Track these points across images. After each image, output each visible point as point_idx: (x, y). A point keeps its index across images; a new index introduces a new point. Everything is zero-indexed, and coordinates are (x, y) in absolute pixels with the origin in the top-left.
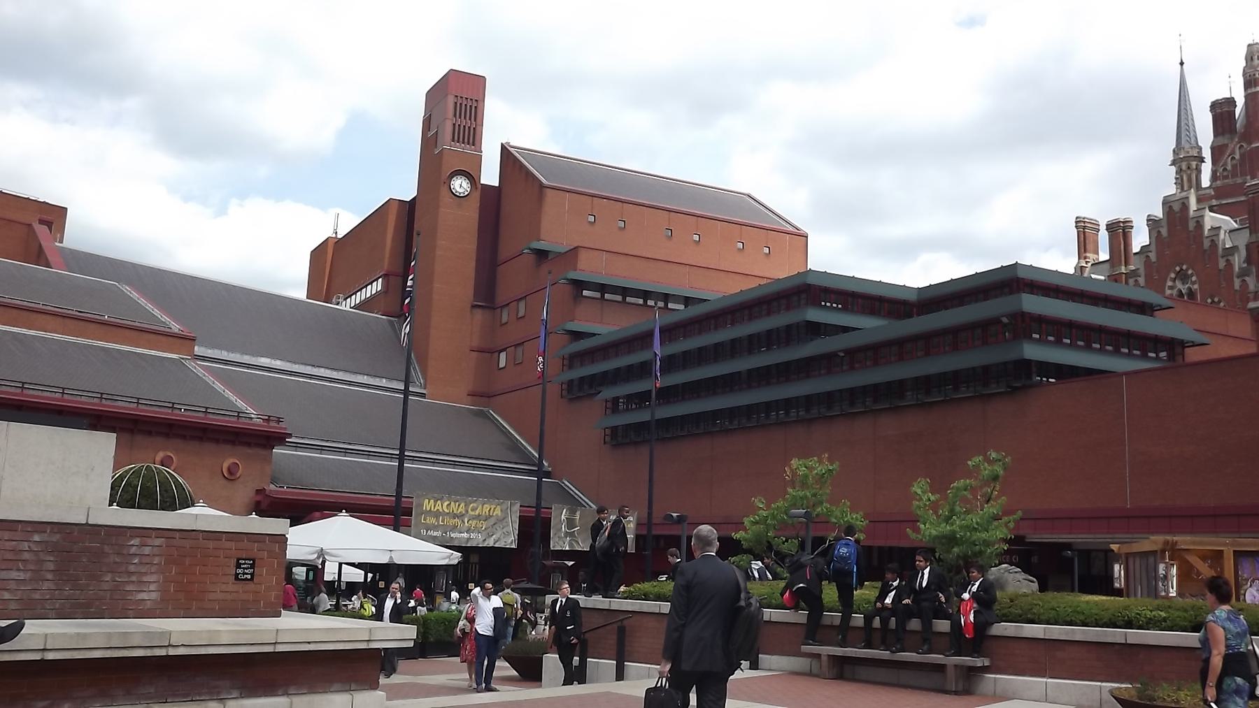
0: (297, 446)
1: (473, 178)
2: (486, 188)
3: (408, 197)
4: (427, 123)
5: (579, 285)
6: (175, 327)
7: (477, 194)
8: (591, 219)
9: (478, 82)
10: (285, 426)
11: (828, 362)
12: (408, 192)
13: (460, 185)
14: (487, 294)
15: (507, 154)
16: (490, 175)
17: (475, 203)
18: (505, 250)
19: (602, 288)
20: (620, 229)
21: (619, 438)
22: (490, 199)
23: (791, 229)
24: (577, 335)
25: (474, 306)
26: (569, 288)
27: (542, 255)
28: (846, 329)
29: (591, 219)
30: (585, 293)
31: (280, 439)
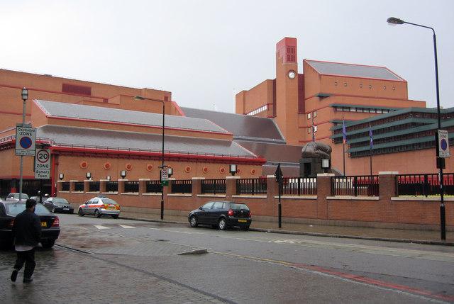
0: (268, 164)
1: (295, 71)
2: (300, 75)
3: (273, 79)
4: (278, 54)
5: (335, 107)
6: (227, 132)
9: (294, 40)
10: (264, 159)
11: (419, 134)
12: (273, 77)
13: (292, 75)
14: (302, 110)
15: (305, 62)
16: (300, 71)
17: (296, 80)
18: (307, 96)
21: (354, 155)
22: (301, 78)
24: (335, 123)
27: (321, 97)
28: (423, 124)
31: (264, 163)
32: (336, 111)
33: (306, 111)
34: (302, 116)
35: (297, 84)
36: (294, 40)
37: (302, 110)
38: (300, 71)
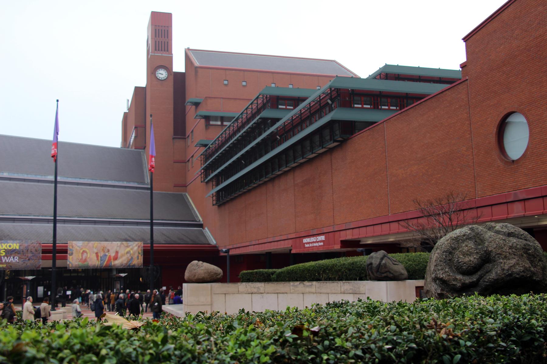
2: (177, 74)
5: (207, 118)
7: (172, 77)
8: (226, 82)
9: (168, 16)
12: (143, 83)
13: (162, 74)
14: (180, 130)
16: (179, 66)
19: (222, 119)
20: (244, 86)
23: (351, 75)
24: (205, 146)
25: (174, 138)
26: (203, 121)
27: (197, 104)
29: (226, 82)
30: (211, 123)
32: (208, 125)
33: (188, 132)
34: (179, 143)
35: (171, 89)
36: (168, 16)
37: (180, 130)
38: (179, 66)
